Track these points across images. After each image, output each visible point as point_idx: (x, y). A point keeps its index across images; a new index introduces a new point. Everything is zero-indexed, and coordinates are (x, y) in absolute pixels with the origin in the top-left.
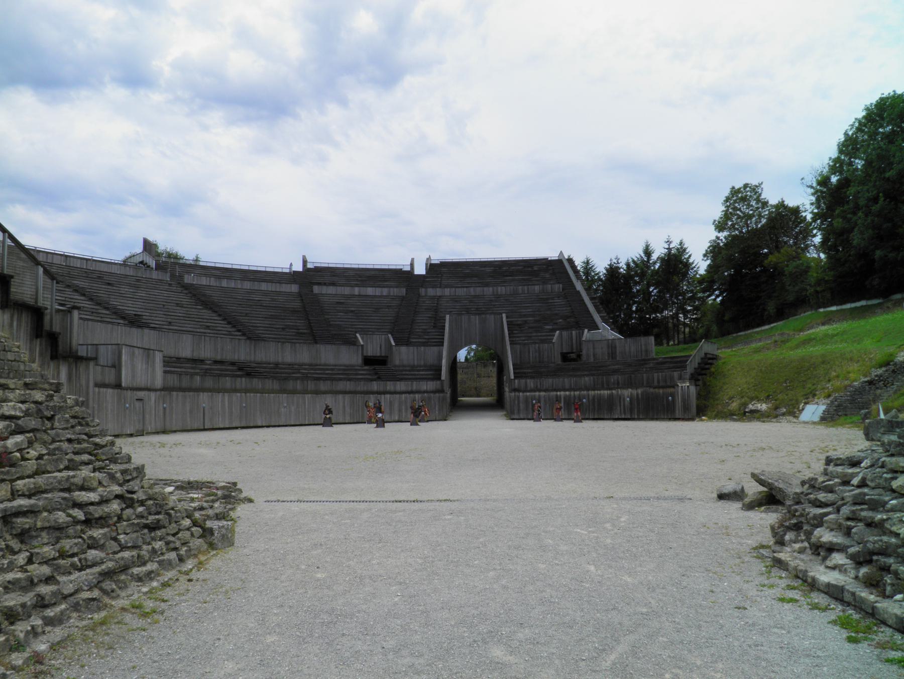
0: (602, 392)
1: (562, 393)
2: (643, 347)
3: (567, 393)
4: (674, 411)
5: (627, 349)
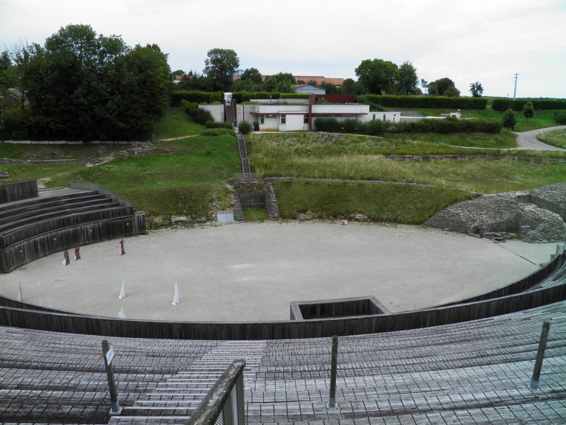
0: (68, 230)
1: (38, 238)
2: (29, 189)
3: (42, 237)
4: (131, 231)
5: (16, 192)
